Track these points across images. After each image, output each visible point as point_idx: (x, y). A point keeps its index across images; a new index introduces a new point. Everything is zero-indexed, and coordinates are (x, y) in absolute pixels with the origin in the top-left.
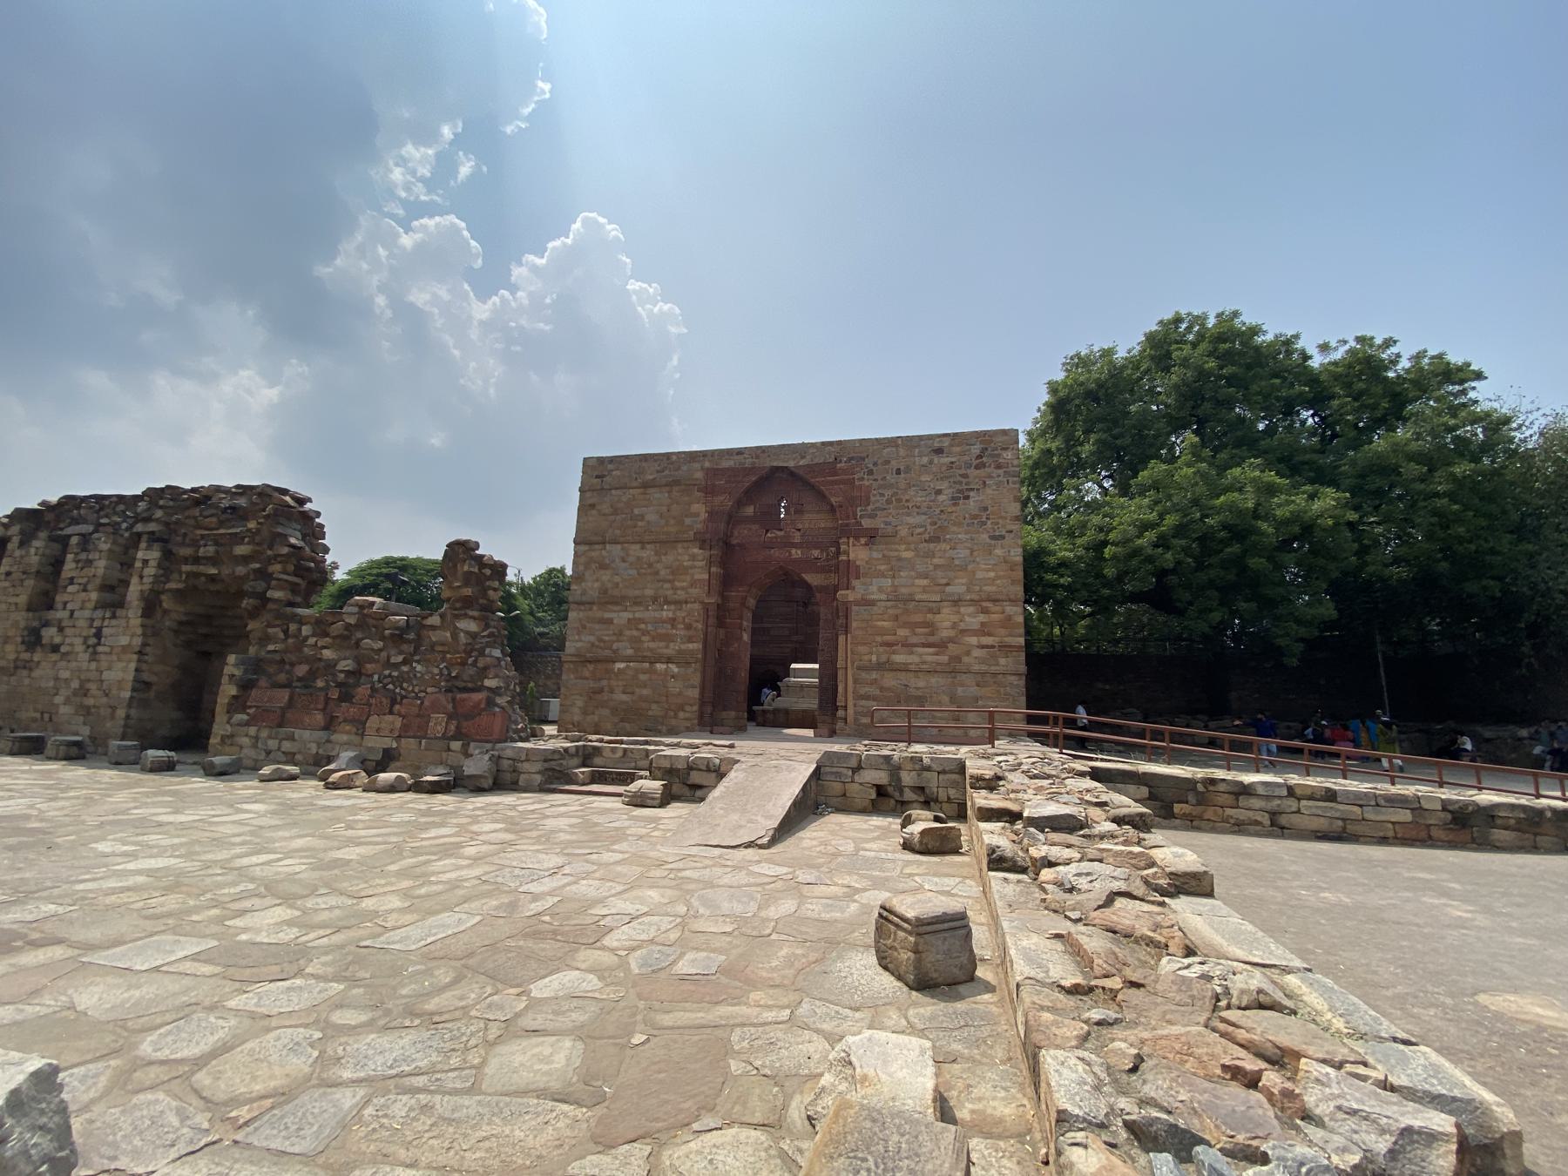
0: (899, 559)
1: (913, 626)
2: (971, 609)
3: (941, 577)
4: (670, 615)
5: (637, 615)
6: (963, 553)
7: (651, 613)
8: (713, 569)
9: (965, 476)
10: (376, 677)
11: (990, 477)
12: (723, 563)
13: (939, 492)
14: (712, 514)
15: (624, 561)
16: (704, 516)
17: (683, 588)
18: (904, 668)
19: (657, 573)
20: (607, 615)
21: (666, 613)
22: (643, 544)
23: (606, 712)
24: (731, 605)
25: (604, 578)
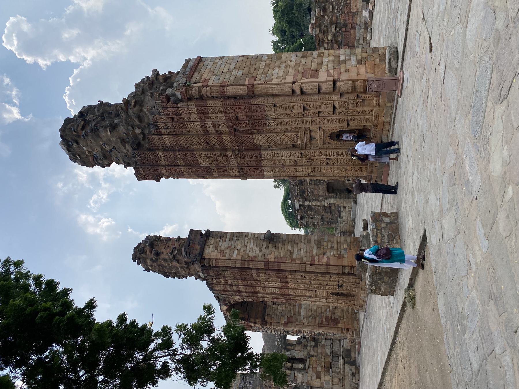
10: (338, 15)
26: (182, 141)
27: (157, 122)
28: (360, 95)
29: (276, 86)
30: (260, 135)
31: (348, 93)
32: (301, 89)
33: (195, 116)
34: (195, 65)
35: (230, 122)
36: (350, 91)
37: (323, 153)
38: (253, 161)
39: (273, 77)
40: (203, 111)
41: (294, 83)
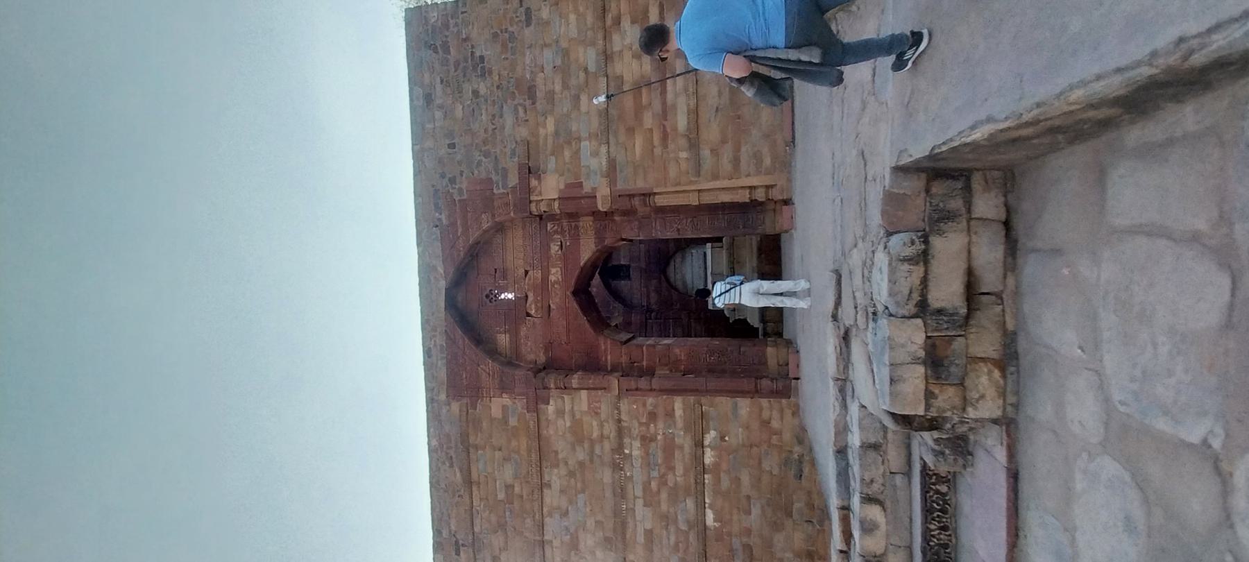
0: (557, 133)
1: (639, 110)
2: (616, 38)
3: (578, 78)
4: (637, 444)
5: (639, 492)
6: (548, 54)
7: (636, 472)
8: (575, 381)
9: (457, 65)
11: (459, 32)
12: (569, 371)
13: (476, 93)
14: (504, 388)
15: (565, 514)
16: (506, 400)
17: (601, 426)
18: (695, 113)
19: (581, 464)
20: (641, 539)
21: (635, 449)
22: (543, 486)
23: (779, 539)
24: (624, 359)
25: (590, 542)
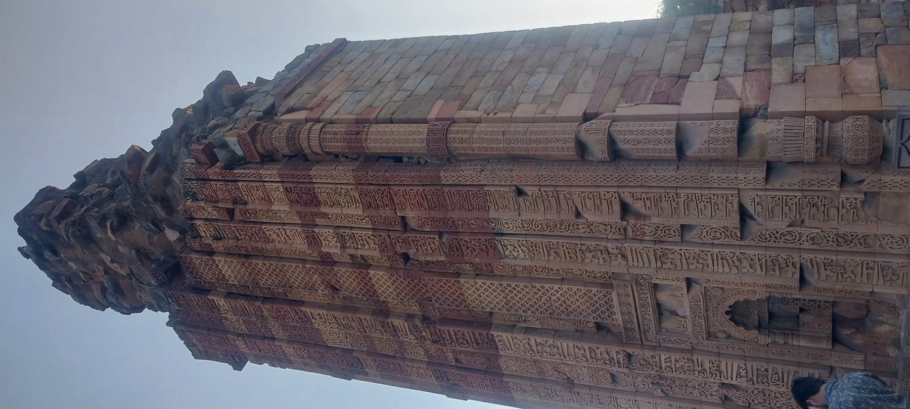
26: (266, 274)
27: (193, 219)
28: (854, 175)
29: (521, 127)
30: (480, 281)
31: (797, 163)
32: (612, 141)
33: (281, 207)
34: (322, 61)
35: (384, 234)
36: (810, 156)
37: (707, 365)
38: (473, 354)
39: (524, 97)
40: (305, 197)
41: (587, 117)
